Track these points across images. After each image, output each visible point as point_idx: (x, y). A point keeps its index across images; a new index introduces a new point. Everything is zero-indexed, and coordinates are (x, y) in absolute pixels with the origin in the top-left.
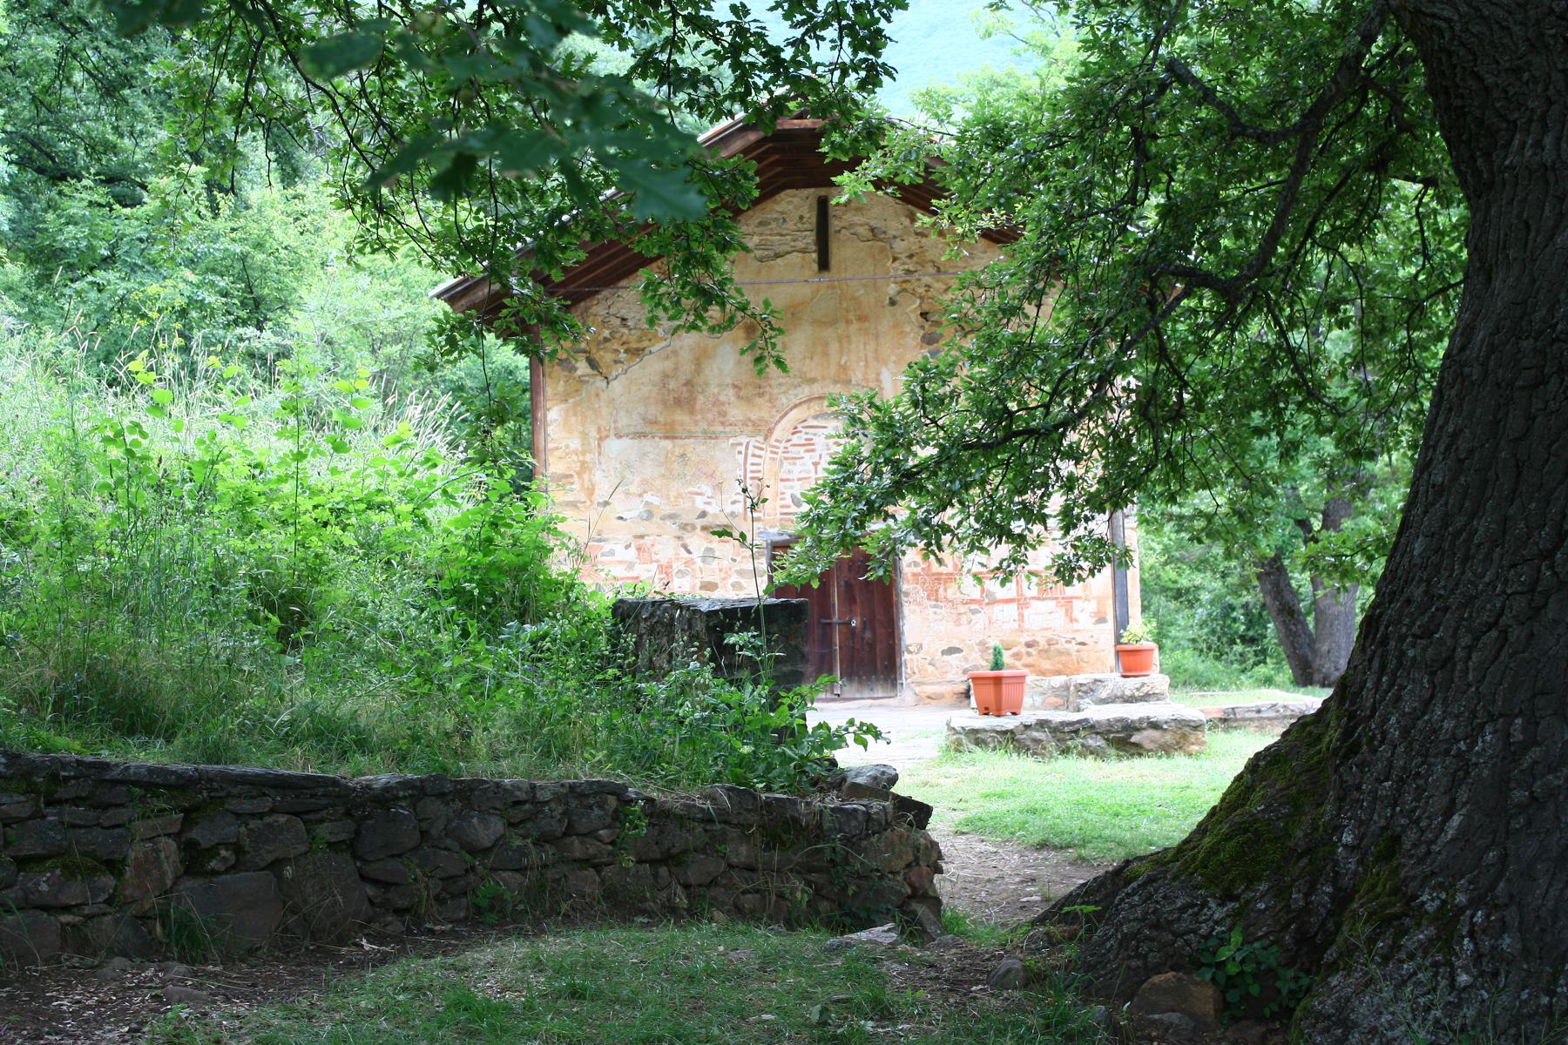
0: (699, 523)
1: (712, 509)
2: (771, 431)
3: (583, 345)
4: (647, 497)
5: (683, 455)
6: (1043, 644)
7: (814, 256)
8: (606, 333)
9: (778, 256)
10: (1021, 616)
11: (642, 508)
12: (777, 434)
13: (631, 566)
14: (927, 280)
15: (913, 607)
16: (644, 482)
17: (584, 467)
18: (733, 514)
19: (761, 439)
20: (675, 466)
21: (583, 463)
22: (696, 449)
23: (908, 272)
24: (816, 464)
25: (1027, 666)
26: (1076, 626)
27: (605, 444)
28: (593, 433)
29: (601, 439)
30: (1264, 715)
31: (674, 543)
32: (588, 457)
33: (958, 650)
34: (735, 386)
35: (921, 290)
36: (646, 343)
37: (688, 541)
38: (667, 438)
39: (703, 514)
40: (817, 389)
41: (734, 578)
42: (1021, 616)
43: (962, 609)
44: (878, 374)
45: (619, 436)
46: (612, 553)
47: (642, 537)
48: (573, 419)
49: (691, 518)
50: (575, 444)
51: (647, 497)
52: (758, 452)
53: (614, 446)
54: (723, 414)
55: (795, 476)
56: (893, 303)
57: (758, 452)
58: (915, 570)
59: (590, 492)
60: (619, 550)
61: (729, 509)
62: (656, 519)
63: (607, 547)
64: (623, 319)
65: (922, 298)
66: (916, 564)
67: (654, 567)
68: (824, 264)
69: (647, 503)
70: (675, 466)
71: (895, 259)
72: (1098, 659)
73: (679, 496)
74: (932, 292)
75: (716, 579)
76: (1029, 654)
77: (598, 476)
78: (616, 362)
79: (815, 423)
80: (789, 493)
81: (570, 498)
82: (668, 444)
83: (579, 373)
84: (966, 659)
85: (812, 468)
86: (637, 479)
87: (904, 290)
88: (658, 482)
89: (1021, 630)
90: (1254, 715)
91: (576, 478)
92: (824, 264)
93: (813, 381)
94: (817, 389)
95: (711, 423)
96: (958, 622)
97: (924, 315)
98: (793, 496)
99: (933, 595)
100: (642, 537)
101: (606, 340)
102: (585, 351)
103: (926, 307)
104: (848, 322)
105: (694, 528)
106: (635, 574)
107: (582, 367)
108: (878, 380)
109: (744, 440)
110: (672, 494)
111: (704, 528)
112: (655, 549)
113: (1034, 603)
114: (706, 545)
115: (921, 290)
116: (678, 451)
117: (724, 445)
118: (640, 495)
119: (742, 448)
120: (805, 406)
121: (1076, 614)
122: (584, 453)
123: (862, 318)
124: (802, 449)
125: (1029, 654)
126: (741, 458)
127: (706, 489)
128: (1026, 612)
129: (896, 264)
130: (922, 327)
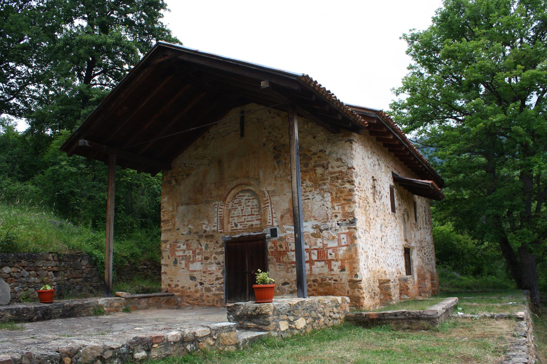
0: (204, 235)
1: (208, 229)
2: (225, 199)
3: (174, 175)
4: (190, 226)
5: (199, 210)
6: (319, 280)
7: (239, 132)
8: (180, 170)
9: (228, 134)
10: (311, 268)
11: (188, 230)
12: (228, 200)
13: (184, 252)
15: (271, 265)
16: (189, 221)
17: (173, 217)
18: (214, 231)
19: (222, 202)
21: (172, 215)
23: (270, 133)
24: (242, 210)
25: (313, 290)
26: (332, 273)
28: (175, 205)
29: (177, 206)
30: (399, 317)
31: (197, 242)
32: (174, 213)
33: (288, 283)
34: (215, 183)
35: (274, 139)
37: (201, 242)
38: (195, 204)
39: (205, 231)
40: (239, 181)
41: (214, 255)
42: (311, 268)
43: (289, 266)
44: (259, 173)
45: (182, 205)
46: (179, 247)
47: (187, 241)
48: (170, 200)
49: (201, 233)
50: (171, 209)
51: (190, 226)
52: (221, 207)
53: (181, 208)
54: (211, 194)
55: (236, 215)
56: (264, 145)
57: (221, 207)
58: (272, 250)
59: (174, 225)
60: (181, 245)
61: (213, 229)
62: (192, 234)
63: (179, 245)
64: (185, 164)
66: (272, 248)
67: (191, 252)
68: (242, 135)
69: (190, 228)
71: (265, 129)
72: (342, 287)
73: (198, 225)
75: (208, 255)
76: (314, 285)
77: (177, 219)
78: (182, 179)
79: (242, 195)
80: (233, 222)
81: (169, 228)
82: (195, 206)
83: (173, 184)
84: (291, 287)
85: (241, 212)
86: (187, 220)
88: (192, 221)
89: (311, 274)
90: (393, 317)
91: (171, 221)
92: (242, 135)
93: (237, 178)
94: (239, 181)
96: (288, 272)
98: (235, 223)
99: (278, 260)
100: (187, 241)
101: (180, 172)
102: (175, 177)
105: (202, 236)
106: (185, 254)
107: (174, 183)
108: (259, 175)
109: (217, 203)
110: (196, 225)
111: (206, 237)
112: (192, 244)
113: (316, 263)
114: (206, 243)
117: (211, 205)
118: (187, 226)
120: (237, 188)
121: (333, 267)
122: (173, 212)
124: (237, 205)
125: (314, 285)
126: (216, 210)
127: (206, 222)
128: (313, 267)
129: (265, 130)
130: (274, 153)
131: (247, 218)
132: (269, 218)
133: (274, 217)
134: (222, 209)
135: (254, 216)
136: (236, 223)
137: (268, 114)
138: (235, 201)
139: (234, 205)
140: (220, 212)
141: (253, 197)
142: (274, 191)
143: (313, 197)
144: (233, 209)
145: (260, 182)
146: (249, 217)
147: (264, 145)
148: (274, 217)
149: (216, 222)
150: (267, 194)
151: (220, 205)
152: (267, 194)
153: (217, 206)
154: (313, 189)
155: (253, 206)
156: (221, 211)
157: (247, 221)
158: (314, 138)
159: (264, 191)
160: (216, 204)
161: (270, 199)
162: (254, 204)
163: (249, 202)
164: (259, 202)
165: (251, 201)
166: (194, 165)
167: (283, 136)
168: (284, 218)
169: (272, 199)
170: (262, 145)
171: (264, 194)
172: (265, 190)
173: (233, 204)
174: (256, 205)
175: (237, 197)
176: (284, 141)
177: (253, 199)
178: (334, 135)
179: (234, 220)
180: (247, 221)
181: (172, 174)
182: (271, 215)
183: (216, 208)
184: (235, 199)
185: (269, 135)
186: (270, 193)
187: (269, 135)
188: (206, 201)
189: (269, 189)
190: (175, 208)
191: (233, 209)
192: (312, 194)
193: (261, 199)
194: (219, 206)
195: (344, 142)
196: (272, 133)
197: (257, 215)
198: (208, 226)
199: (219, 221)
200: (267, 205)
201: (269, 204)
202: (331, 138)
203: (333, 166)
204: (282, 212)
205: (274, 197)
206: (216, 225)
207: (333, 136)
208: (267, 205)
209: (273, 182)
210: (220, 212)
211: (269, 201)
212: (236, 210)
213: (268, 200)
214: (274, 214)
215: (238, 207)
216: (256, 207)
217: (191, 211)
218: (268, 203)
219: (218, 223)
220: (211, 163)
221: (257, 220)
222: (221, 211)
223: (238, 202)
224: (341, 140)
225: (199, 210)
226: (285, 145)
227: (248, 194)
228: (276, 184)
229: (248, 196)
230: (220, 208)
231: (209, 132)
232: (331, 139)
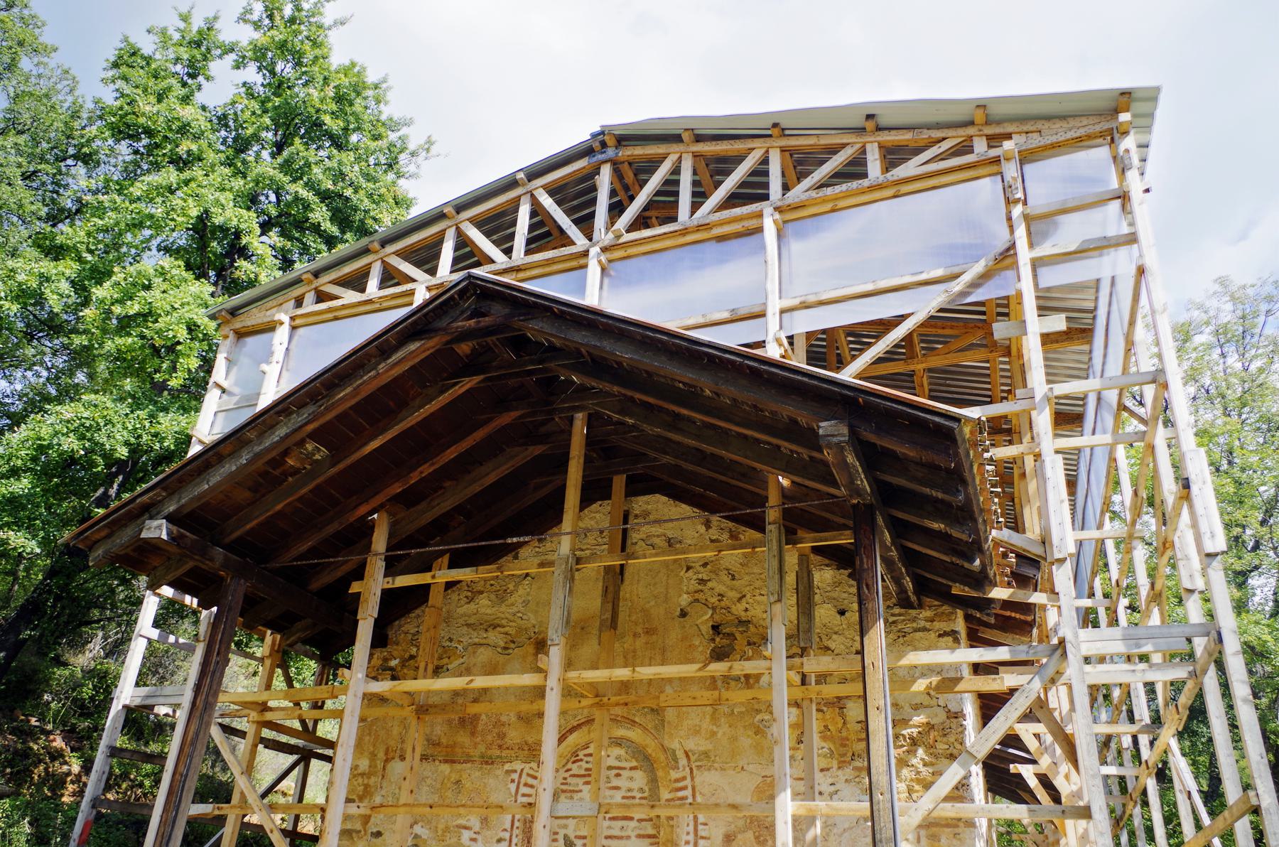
4: (418, 829)
5: (458, 782)
14: (720, 588)
20: (449, 794)
21: (366, 786)
22: (471, 775)
23: (702, 582)
27: (389, 766)
28: (381, 755)
29: (387, 761)
32: (372, 780)
35: (714, 600)
36: (446, 661)
38: (446, 761)
51: (418, 829)
54: (502, 736)
56: (683, 614)
57: (530, 781)
65: (714, 609)
69: (416, 836)
70: (449, 794)
71: (688, 568)
73: (447, 829)
74: (725, 602)
80: (562, 832)
82: (445, 768)
87: (697, 601)
95: (488, 748)
97: (715, 628)
98: (566, 837)
103: (717, 617)
104: (635, 635)
109: (518, 766)
110: (441, 826)
115: (714, 600)
116: (454, 777)
117: (499, 772)
119: (515, 776)
120: (585, 729)
123: (649, 632)
124: (580, 781)
126: (513, 787)
127: (477, 827)
129: (690, 573)
131: (609, 827)
132: (685, 838)
133: (702, 838)
134: (532, 786)
135: (633, 824)
136: (572, 837)
137: (702, 529)
138: (575, 769)
139: (569, 780)
140: (524, 795)
141: (634, 764)
142: (706, 754)
143: (833, 789)
144: (563, 791)
145: (663, 721)
146: (614, 823)
147: (683, 614)
148: (702, 838)
149: (508, 826)
150: (683, 762)
151: (528, 775)
152: (683, 762)
153: (515, 776)
154: (835, 764)
155: (629, 790)
156: (529, 796)
157: (607, 837)
158: (842, 613)
159: (674, 751)
160: (515, 771)
161: (692, 778)
162: (635, 785)
163: (618, 775)
164: (653, 781)
165: (625, 773)
166: (460, 642)
167: (744, 596)
168: (734, 843)
169: (698, 780)
170: (678, 613)
171: (676, 760)
172: (675, 745)
173: (567, 775)
174: (641, 790)
175: (581, 756)
176: (746, 610)
177: (631, 769)
178: (903, 611)
179: (565, 827)
180: (607, 837)
181: (386, 660)
182: (691, 828)
183: (513, 781)
184: (574, 762)
185: (700, 587)
186: (693, 758)
187: (700, 587)
188: (482, 756)
189: (691, 745)
190: (380, 765)
191: (563, 791)
192: (831, 781)
193: (660, 773)
194: (524, 775)
195: (933, 635)
196: (710, 584)
197: (640, 821)
198: (479, 837)
199: (517, 824)
200: (681, 794)
201: (688, 793)
202: (891, 619)
203: (901, 703)
204: (730, 823)
205: (706, 773)
206: (507, 835)
207: (900, 615)
208: (681, 794)
209: (706, 725)
210: (524, 795)
211: (688, 782)
212: (576, 796)
213: (684, 778)
214: (700, 827)
215: (581, 787)
216: (639, 795)
217: (429, 781)
218: (684, 788)
219: (516, 832)
220: (512, 645)
221: (639, 836)
222: (529, 796)
223: (583, 772)
224: (924, 629)
225: (458, 782)
226: (747, 623)
227: (618, 751)
228: (714, 734)
229: (618, 758)
230: (526, 785)
231: (516, 557)
232: (894, 622)
